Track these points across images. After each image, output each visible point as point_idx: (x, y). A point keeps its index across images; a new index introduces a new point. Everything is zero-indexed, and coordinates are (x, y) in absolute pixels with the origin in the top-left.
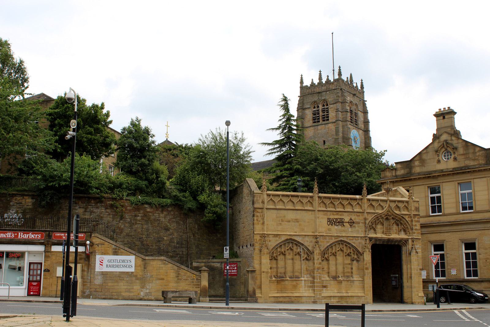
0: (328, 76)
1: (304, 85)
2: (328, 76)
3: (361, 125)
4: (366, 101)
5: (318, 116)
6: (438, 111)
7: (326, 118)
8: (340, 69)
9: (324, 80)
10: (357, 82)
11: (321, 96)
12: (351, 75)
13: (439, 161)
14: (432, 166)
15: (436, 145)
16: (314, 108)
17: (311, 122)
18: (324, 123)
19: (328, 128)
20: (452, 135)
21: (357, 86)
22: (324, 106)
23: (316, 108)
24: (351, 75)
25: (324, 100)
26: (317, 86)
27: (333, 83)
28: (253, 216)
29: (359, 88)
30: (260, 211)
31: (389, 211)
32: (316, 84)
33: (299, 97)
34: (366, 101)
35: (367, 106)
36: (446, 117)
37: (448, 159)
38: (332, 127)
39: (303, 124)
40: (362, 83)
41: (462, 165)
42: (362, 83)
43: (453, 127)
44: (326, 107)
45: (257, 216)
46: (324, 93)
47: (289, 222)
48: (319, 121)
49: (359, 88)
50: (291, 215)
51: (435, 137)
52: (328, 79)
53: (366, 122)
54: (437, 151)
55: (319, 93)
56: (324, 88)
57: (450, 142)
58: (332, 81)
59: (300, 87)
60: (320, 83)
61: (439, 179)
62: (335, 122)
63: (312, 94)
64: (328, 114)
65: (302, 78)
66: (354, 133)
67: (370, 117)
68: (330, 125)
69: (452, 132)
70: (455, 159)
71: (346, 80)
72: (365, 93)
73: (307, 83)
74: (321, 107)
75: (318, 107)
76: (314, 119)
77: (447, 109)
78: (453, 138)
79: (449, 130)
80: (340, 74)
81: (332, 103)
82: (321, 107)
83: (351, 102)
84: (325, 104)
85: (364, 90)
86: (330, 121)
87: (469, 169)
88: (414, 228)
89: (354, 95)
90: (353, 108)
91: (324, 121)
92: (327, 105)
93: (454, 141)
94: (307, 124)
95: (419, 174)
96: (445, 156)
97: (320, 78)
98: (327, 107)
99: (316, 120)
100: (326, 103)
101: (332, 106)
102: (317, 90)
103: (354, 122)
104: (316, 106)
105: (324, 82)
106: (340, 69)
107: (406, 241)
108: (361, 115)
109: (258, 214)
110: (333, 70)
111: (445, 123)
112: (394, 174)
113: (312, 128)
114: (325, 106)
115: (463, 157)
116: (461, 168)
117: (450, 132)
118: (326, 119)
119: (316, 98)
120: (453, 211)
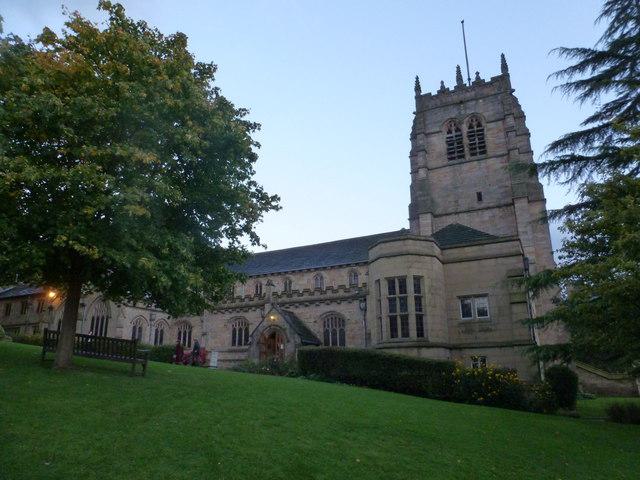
5: (458, 147)
7: (480, 149)
11: (465, 109)
19: (487, 168)
22: (471, 127)
23: (454, 132)
25: (474, 115)
26: (453, 92)
27: (490, 83)
46: (474, 102)
48: (463, 156)
55: (461, 102)
59: (416, 98)
60: (460, 86)
63: (445, 106)
65: (417, 82)
68: (491, 161)
73: (430, 88)
74: (465, 129)
75: (458, 130)
76: (450, 153)
81: (493, 119)
82: (465, 129)
86: (490, 152)
91: (472, 155)
92: (479, 125)
102: (456, 98)
104: (453, 128)
113: (448, 169)
119: (453, 113)
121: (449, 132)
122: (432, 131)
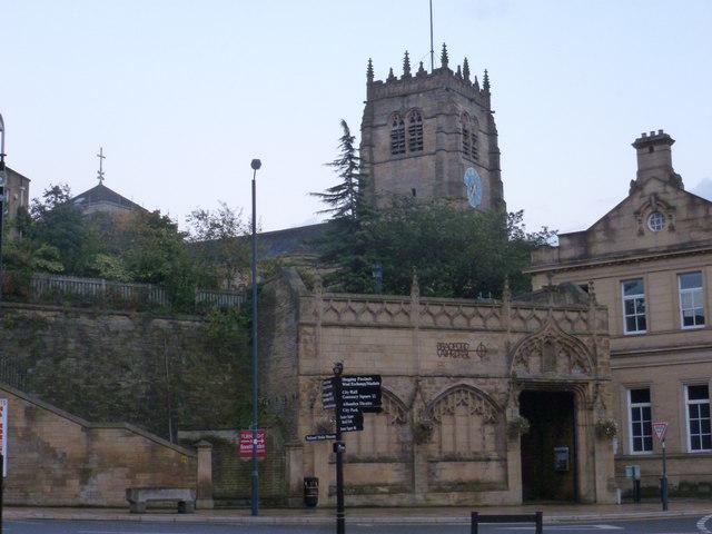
0: (421, 63)
1: (375, 80)
2: (421, 63)
3: (484, 159)
6: (640, 137)
7: (417, 145)
8: (445, 51)
9: (414, 72)
10: (476, 75)
11: (409, 101)
12: (466, 61)
13: (641, 233)
14: (628, 242)
15: (637, 203)
16: (395, 125)
17: (388, 151)
18: (412, 154)
20: (665, 183)
21: (477, 83)
22: (413, 121)
24: (466, 61)
25: (415, 110)
27: (431, 76)
28: (298, 341)
29: (481, 87)
30: (310, 330)
31: (552, 329)
32: (399, 78)
35: (496, 121)
36: (655, 148)
37: (659, 228)
38: (429, 162)
39: (372, 157)
40: (486, 76)
41: (685, 240)
42: (486, 76)
43: (668, 167)
44: (417, 123)
45: (306, 341)
46: (414, 96)
47: (366, 351)
49: (481, 87)
50: (368, 337)
51: (636, 187)
52: (421, 69)
53: (494, 153)
54: (637, 213)
55: (405, 96)
56: (413, 87)
57: (662, 196)
58: (430, 72)
59: (368, 84)
60: (407, 76)
61: (642, 265)
62: (434, 154)
63: (391, 97)
65: (370, 66)
66: (472, 175)
67: (501, 143)
69: (667, 178)
70: (672, 229)
71: (455, 71)
72: (492, 98)
73: (381, 76)
74: (407, 124)
75: (402, 123)
77: (657, 133)
78: (669, 189)
79: (659, 173)
80: (445, 59)
81: (429, 115)
82: (407, 124)
83: (465, 114)
85: (491, 90)
87: (698, 247)
88: (599, 360)
89: (471, 100)
90: (470, 125)
91: (413, 150)
92: (420, 120)
93: (670, 196)
94: (378, 157)
95: (605, 255)
96: (652, 223)
97: (407, 67)
99: (397, 148)
100: (417, 116)
101: (427, 122)
102: (401, 89)
103: (471, 152)
104: (398, 121)
105: (414, 75)
106: (445, 51)
107: (585, 384)
108: (483, 140)
109: (308, 337)
110: (432, 52)
111: (655, 159)
112: (556, 257)
115: (688, 225)
116: (683, 246)
117: (662, 178)
118: (417, 146)
119: (397, 106)
120: (668, 326)
121: (395, 125)
122: (380, 123)
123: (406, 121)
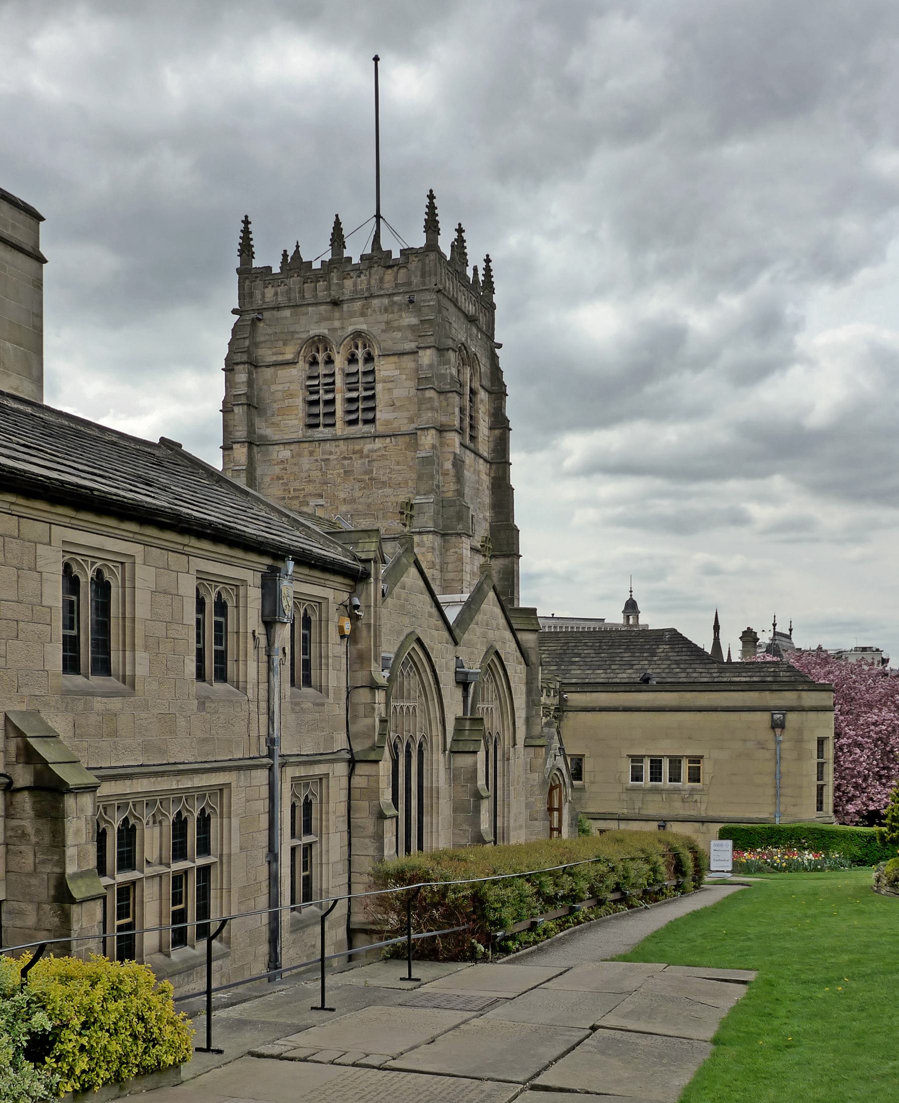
1: (257, 263)
4: (500, 346)
22: (352, 360)
25: (358, 334)
33: (234, 312)
34: (500, 346)
48: (334, 425)
64: (370, 393)
75: (330, 361)
84: (360, 353)
92: (369, 358)
98: (369, 367)
105: (356, 260)
110: (378, 216)
114: (361, 362)
123: (340, 361)
